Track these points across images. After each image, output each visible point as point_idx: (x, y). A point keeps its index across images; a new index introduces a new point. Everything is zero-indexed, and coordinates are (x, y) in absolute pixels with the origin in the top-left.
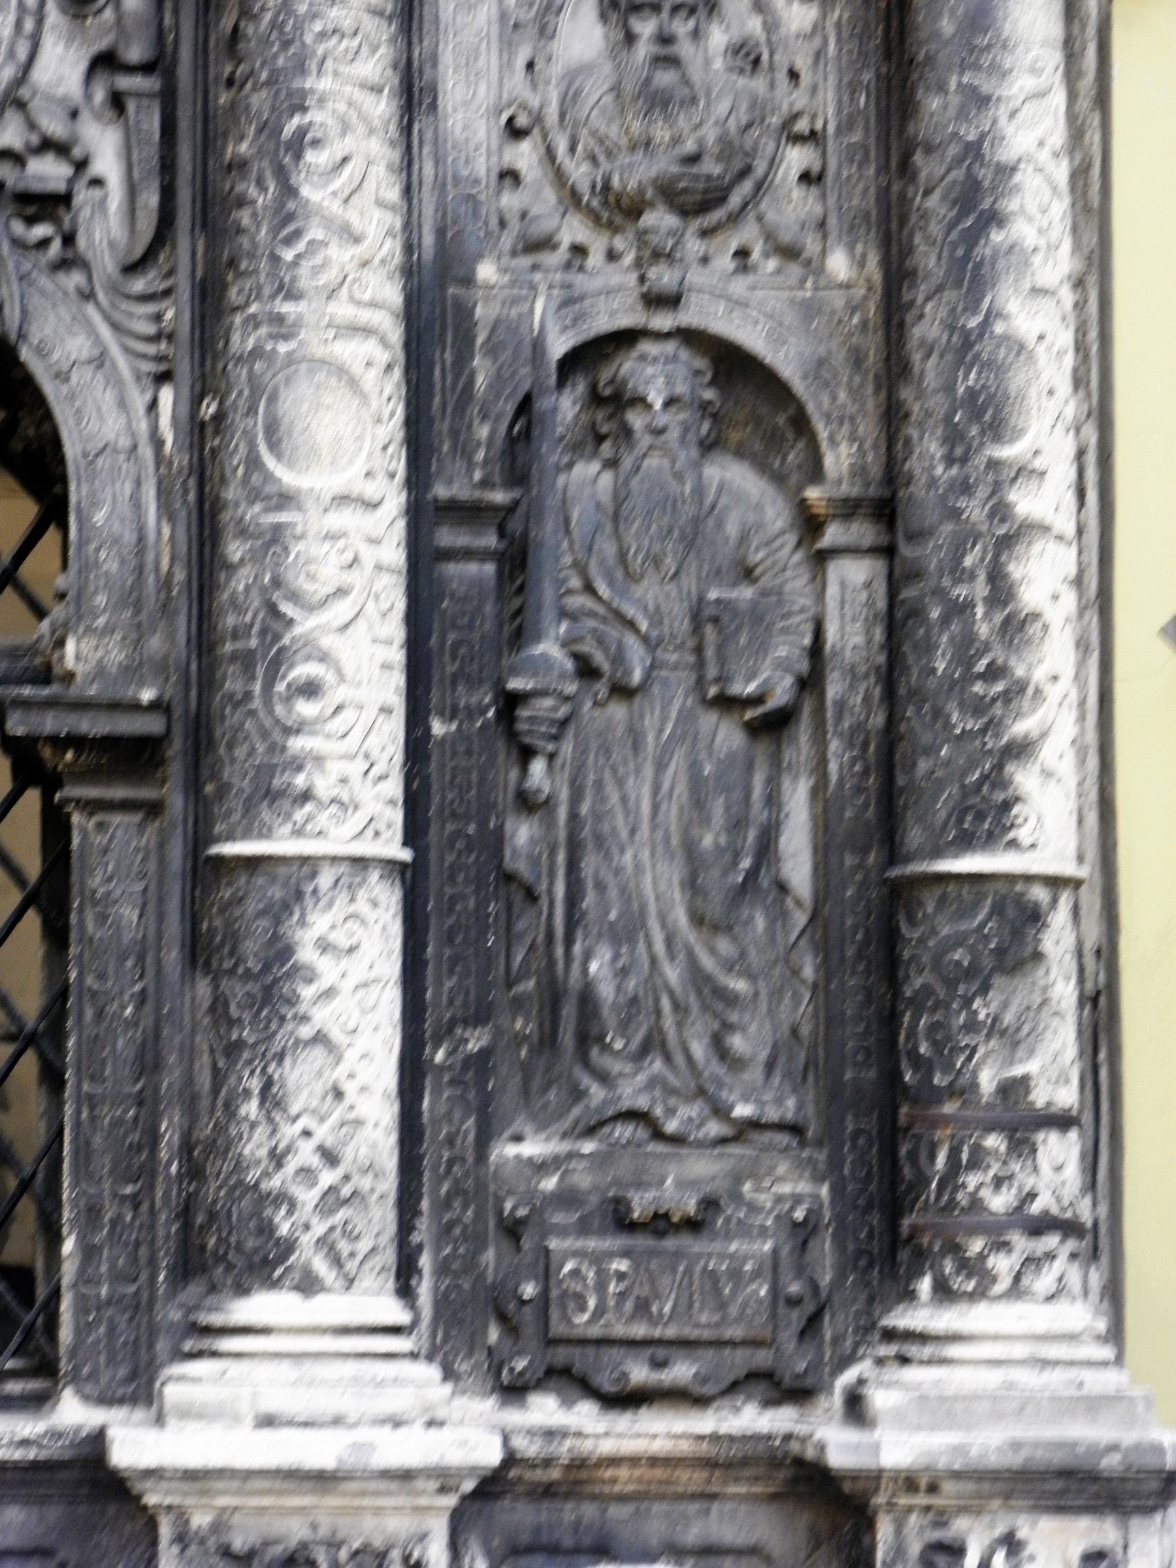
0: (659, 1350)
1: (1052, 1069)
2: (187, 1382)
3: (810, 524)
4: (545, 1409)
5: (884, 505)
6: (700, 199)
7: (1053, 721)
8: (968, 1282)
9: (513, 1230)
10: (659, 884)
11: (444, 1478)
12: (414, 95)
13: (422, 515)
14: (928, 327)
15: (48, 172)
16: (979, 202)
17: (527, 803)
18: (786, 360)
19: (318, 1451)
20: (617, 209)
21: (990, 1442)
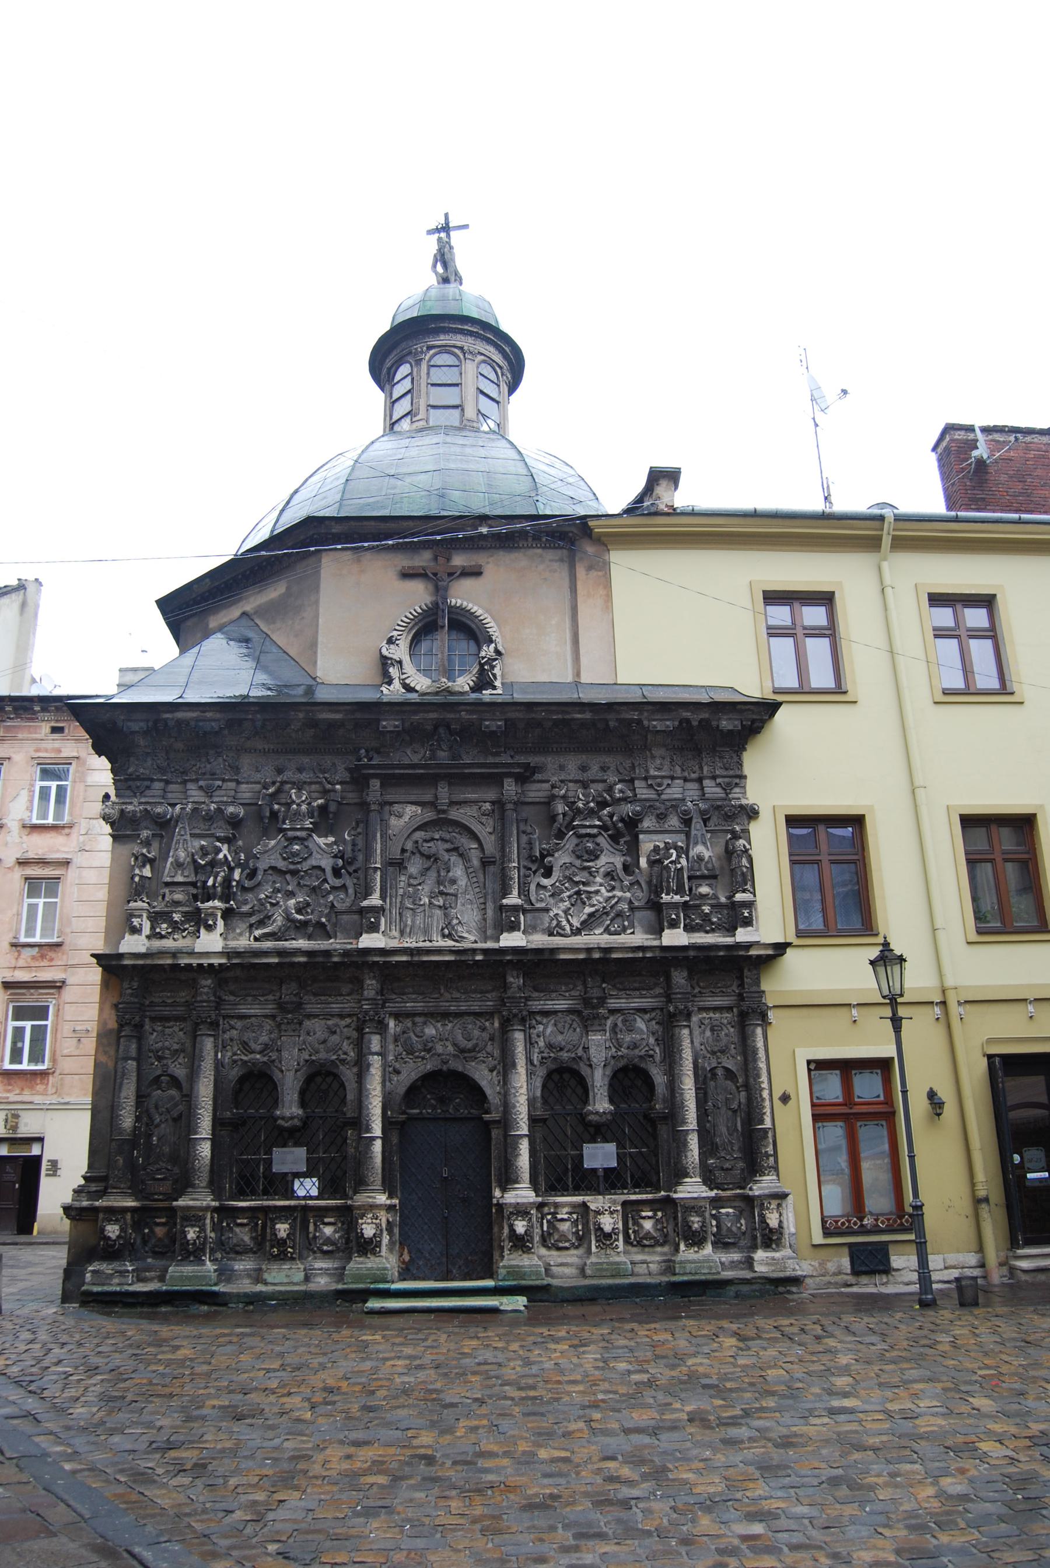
0: (728, 1184)
1: (770, 1150)
2: (680, 1188)
3: (738, 1088)
4: (715, 1191)
5: (747, 1086)
6: (722, 1052)
7: (768, 1110)
8: (763, 1174)
9: (710, 1171)
10: (724, 1130)
11: (708, 1198)
12: (692, 1042)
13: (696, 1089)
14: (750, 1066)
15: (651, 1052)
16: (755, 1052)
17: (709, 1121)
18: (734, 1069)
19: (695, 1195)
20: (713, 1053)
21: (766, 1192)
